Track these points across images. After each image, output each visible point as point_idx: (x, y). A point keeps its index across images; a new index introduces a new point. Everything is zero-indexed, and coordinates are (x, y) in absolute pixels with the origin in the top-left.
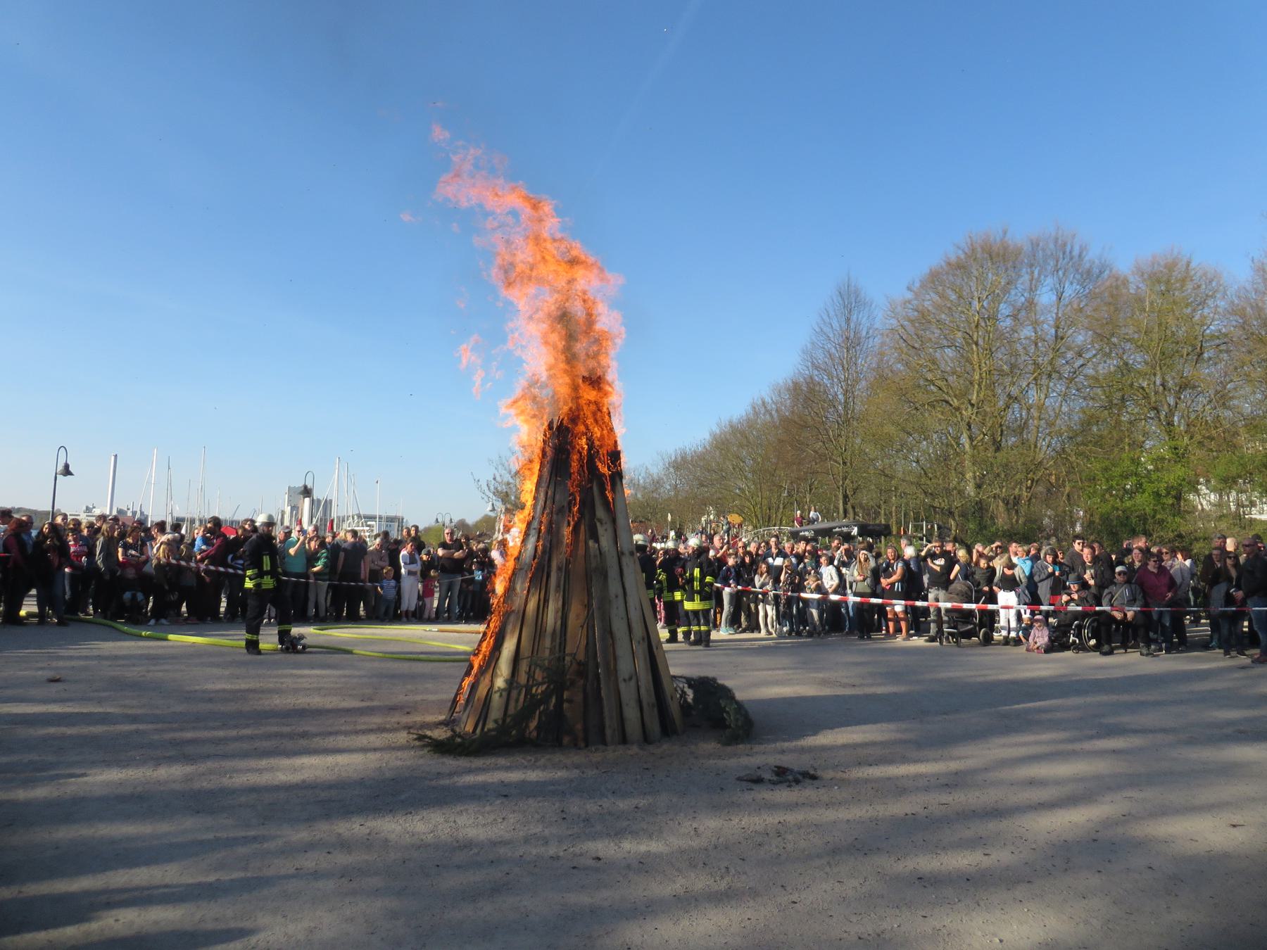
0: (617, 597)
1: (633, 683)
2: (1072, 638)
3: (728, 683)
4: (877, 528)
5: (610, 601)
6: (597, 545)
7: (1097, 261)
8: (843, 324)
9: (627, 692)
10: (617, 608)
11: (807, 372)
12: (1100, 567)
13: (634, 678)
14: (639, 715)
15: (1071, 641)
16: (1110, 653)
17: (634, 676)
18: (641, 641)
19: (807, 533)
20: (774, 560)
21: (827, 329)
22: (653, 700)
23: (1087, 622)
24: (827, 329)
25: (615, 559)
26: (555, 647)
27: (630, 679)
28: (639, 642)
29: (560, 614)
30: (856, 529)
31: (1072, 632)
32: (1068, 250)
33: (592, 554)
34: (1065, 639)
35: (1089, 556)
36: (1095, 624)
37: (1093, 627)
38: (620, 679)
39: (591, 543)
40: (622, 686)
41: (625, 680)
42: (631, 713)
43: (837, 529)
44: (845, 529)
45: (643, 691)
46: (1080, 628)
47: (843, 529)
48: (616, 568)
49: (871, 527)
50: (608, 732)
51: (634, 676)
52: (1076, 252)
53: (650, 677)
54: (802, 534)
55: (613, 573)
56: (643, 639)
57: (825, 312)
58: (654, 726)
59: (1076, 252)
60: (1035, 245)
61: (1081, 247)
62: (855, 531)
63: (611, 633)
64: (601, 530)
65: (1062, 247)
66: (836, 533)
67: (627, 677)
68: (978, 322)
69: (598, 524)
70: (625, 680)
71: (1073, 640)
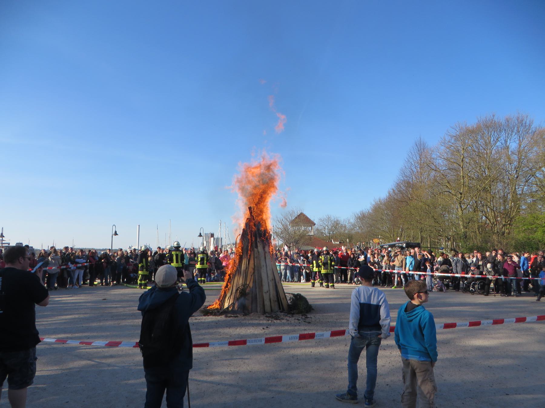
0: (263, 266)
1: (268, 293)
2: (471, 289)
3: (306, 297)
4: (414, 244)
5: (261, 267)
6: (257, 250)
7: (538, 127)
8: (418, 158)
9: (266, 297)
10: (263, 270)
11: (402, 179)
12: (484, 261)
13: (268, 292)
14: (270, 303)
15: (471, 290)
16: (487, 294)
17: (268, 291)
18: (272, 280)
19: (386, 246)
20: (361, 256)
21: (411, 160)
22: (276, 299)
23: (478, 282)
24: (411, 160)
25: (263, 254)
26: (243, 282)
27: (267, 292)
28: (271, 281)
29: (245, 272)
30: (405, 244)
31: (471, 286)
32: (524, 122)
33: (255, 252)
34: (468, 289)
35: (480, 257)
36: (482, 284)
37: (481, 285)
38: (264, 292)
39: (255, 249)
40: (264, 294)
41: (265, 293)
42: (267, 303)
43: (397, 245)
44: (400, 245)
45: (271, 296)
46: (475, 284)
47: (399, 245)
48: (263, 257)
49: (411, 244)
50: (259, 309)
51: (268, 291)
52: (527, 124)
53: (275, 292)
54: (384, 246)
55: (262, 258)
56: (273, 280)
57: (410, 153)
58: (276, 307)
59: (527, 124)
60: (507, 121)
61: (530, 121)
62: (404, 245)
63: (261, 278)
64: (258, 244)
65: (521, 122)
66: (397, 246)
67: (266, 291)
68: (463, 159)
69: (258, 243)
70: (265, 293)
71: (471, 289)
